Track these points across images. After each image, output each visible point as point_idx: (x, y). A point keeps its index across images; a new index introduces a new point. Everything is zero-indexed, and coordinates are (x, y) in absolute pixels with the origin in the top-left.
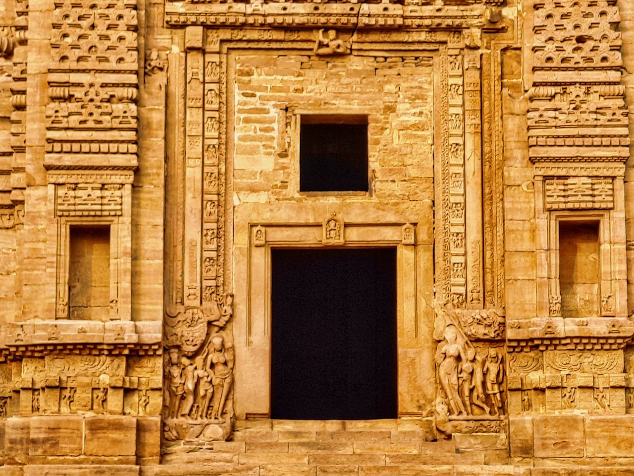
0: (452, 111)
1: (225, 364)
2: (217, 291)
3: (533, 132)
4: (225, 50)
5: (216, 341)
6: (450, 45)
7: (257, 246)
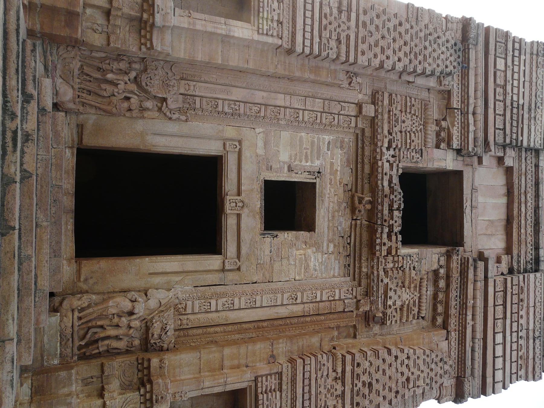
1: (130, 110)
2: (189, 108)
3: (313, 358)
4: (357, 132)
5: (149, 104)
6: (359, 288)
7: (224, 143)
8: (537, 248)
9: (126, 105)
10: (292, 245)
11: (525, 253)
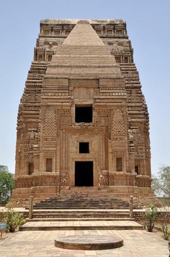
11: (94, 83)
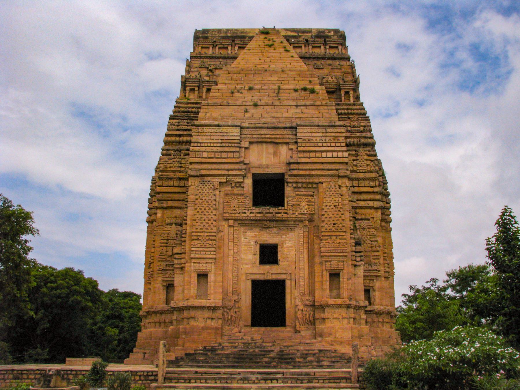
0: (301, 243)
3: (322, 249)
5: (237, 306)
8: (286, 128)
9: (238, 313)
10: (283, 253)
